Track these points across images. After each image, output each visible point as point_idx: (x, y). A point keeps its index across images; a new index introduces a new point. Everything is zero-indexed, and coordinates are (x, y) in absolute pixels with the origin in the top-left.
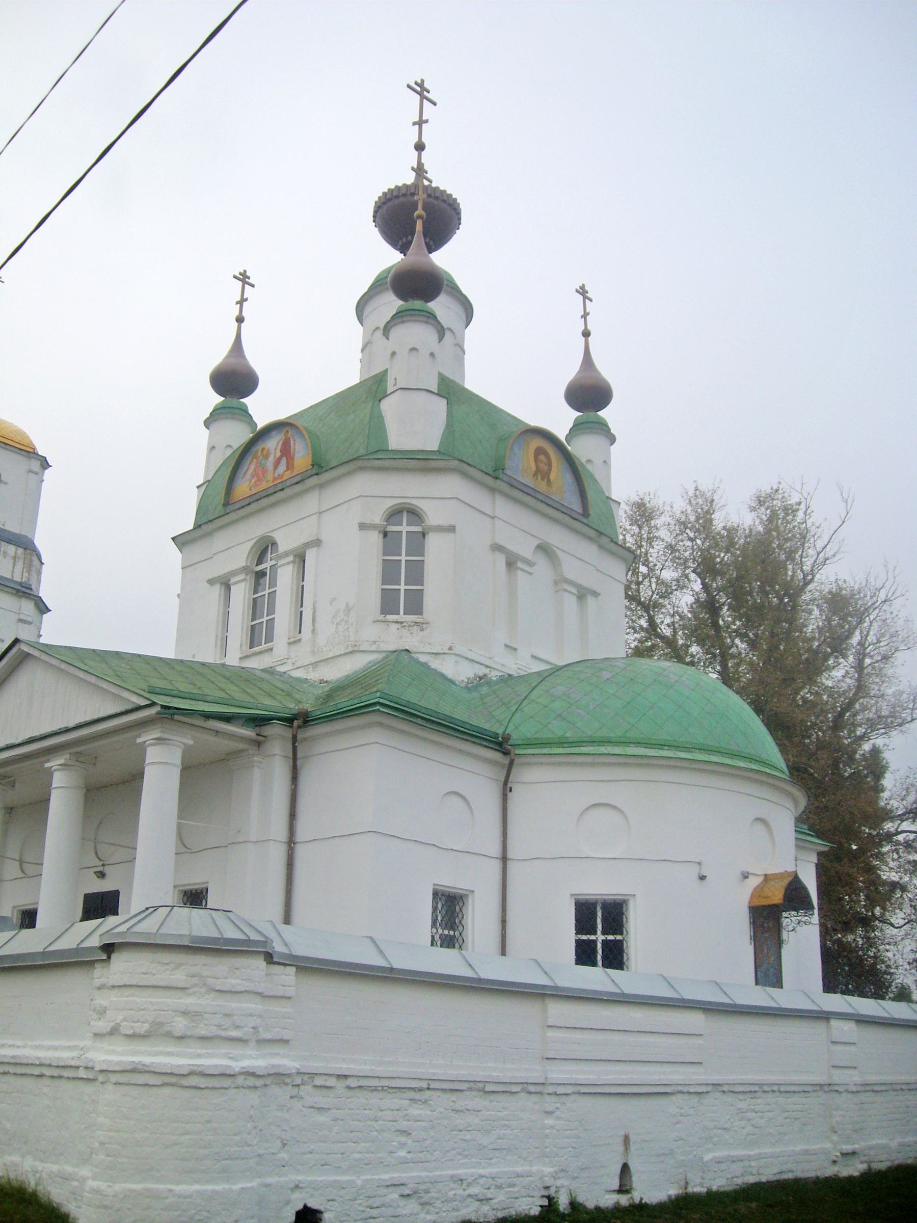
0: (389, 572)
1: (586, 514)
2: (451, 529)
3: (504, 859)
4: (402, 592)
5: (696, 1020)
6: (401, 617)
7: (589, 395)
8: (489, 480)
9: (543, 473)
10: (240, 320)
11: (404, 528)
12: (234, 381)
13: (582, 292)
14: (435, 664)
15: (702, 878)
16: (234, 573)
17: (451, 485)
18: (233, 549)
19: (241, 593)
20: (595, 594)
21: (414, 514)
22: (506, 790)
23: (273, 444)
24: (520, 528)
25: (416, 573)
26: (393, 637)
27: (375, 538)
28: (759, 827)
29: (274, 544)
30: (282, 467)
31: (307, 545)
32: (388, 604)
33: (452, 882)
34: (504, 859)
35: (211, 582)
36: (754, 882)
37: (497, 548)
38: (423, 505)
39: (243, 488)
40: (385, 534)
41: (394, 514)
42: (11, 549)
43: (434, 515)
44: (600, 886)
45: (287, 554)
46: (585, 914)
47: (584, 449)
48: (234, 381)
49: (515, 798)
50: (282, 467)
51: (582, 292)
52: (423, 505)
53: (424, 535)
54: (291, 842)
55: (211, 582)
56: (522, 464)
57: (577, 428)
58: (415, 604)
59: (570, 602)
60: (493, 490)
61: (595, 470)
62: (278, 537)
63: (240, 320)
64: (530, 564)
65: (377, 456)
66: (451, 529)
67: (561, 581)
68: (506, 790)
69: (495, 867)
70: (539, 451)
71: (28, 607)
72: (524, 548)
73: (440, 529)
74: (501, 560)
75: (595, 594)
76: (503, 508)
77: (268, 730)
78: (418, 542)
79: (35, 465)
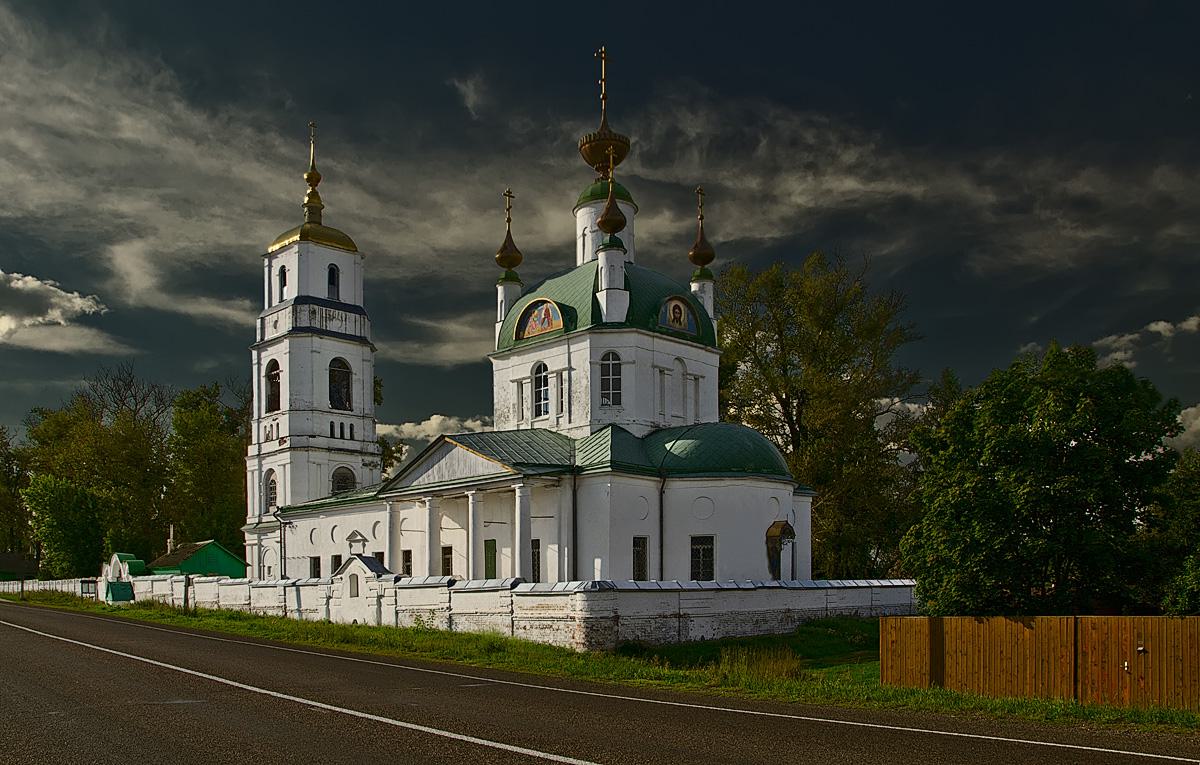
0: (605, 385)
9: (677, 319)
16: (524, 379)
21: (616, 357)
25: (617, 384)
27: (598, 367)
31: (564, 369)
35: (513, 381)
37: (654, 367)
41: (606, 357)
52: (621, 352)
53: (620, 364)
55: (513, 381)
58: (617, 400)
70: (676, 307)
72: (666, 362)
78: (617, 369)
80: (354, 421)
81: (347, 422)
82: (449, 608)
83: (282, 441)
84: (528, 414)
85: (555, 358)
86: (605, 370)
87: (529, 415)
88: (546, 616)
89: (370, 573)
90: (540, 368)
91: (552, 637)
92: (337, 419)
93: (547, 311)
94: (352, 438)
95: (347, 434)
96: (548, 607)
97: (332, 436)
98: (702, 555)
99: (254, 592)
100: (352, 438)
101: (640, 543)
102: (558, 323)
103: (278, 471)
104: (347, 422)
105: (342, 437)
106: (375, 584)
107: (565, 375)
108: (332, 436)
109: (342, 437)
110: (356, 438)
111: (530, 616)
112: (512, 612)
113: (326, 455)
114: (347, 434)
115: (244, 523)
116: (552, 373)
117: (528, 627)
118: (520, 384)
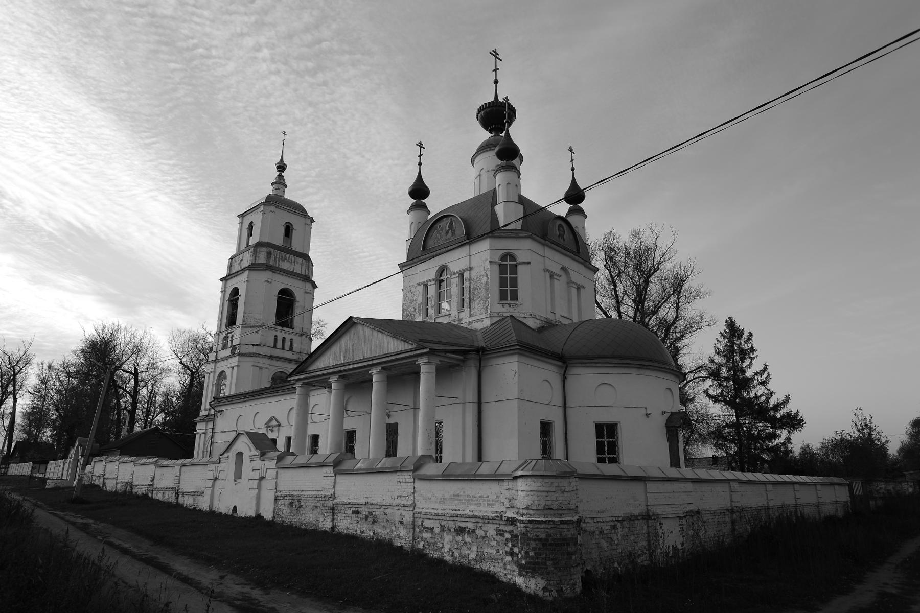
0: (503, 282)
1: (578, 252)
2: (529, 263)
3: (565, 407)
4: (508, 289)
5: (689, 486)
6: (509, 301)
7: (575, 196)
8: (542, 241)
9: (561, 236)
10: (420, 164)
11: (508, 263)
12: (419, 191)
13: (571, 150)
14: (525, 321)
15: (647, 415)
16: (430, 281)
17: (527, 244)
18: (427, 271)
19: (432, 290)
20: (584, 288)
21: (513, 258)
22: (564, 378)
23: (445, 224)
24: (555, 260)
25: (514, 283)
26: (505, 311)
27: (496, 267)
28: (668, 391)
29: (447, 267)
30: (450, 234)
31: (465, 270)
32: (503, 296)
33: (546, 418)
34: (565, 407)
35: (419, 284)
36: (668, 415)
37: (546, 270)
38: (516, 253)
39: (431, 243)
40: (500, 265)
41: (504, 258)
42: (300, 260)
43: (521, 257)
44: (606, 417)
45: (455, 274)
46: (599, 428)
47: (574, 220)
48: (419, 191)
49: (568, 382)
50: (450, 234)
51: (571, 150)
53: (516, 266)
54: (480, 403)
56: (554, 231)
57: (571, 212)
58: (514, 296)
59: (574, 291)
60: (544, 245)
61: (579, 230)
62: (450, 265)
63: (420, 164)
64: (559, 276)
65: (495, 231)
66: (529, 263)
67: (570, 282)
68: (564, 378)
69: (561, 410)
70: (560, 226)
71: (309, 285)
72: (556, 269)
73: (524, 263)
74: (548, 275)
75: (584, 288)
76: (549, 252)
77: (469, 356)
79: (308, 221)
80: (294, 337)
81: (288, 338)
82: (334, 497)
83: (234, 348)
84: (431, 311)
85: (456, 260)
86: (502, 269)
87: (433, 311)
88: (467, 512)
89: (254, 452)
90: (442, 270)
91: (474, 548)
92: (282, 333)
93: (451, 224)
94: (291, 350)
95: (287, 347)
96: (469, 499)
97: (275, 347)
98: (607, 438)
99: (159, 471)
100: (291, 350)
101: (546, 427)
102: (461, 231)
103: (228, 372)
104: (288, 338)
105: (283, 348)
106: (257, 464)
107: (466, 275)
108: (275, 347)
109: (283, 348)
110: (294, 349)
111: (440, 512)
112: (414, 505)
113: (268, 361)
114: (287, 347)
115: (198, 416)
116: (455, 274)
117: (437, 530)
118: (426, 286)
